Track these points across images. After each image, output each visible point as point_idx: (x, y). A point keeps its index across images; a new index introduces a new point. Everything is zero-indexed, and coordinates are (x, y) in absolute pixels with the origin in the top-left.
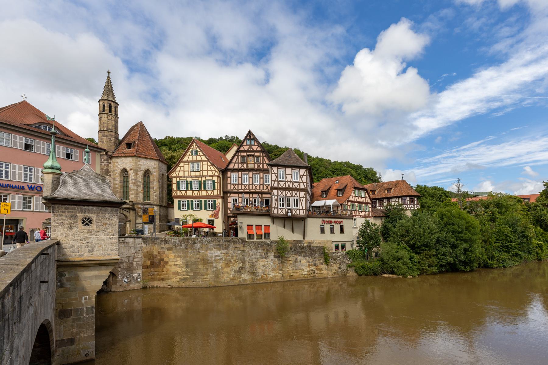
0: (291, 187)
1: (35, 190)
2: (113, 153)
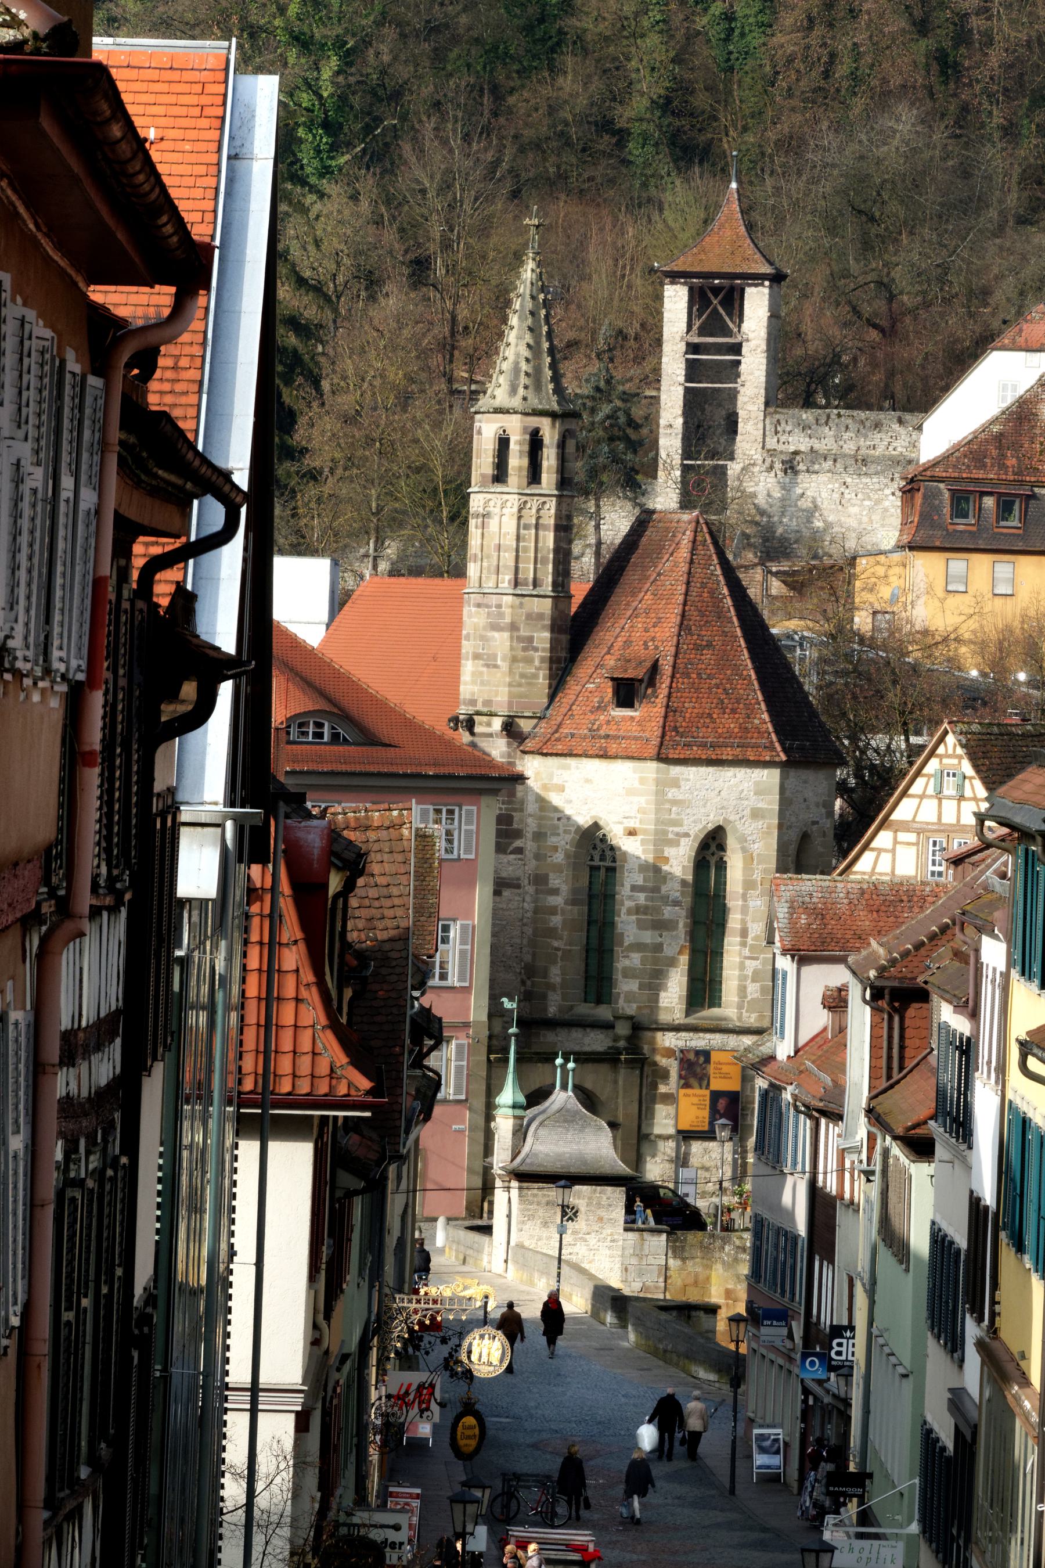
2: (540, 718)
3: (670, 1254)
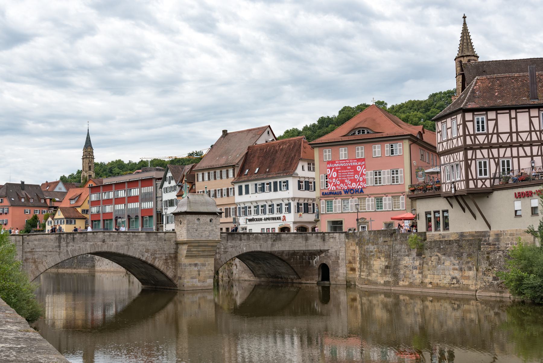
0: (451, 147)
1: (349, 193)
3: (346, 238)
